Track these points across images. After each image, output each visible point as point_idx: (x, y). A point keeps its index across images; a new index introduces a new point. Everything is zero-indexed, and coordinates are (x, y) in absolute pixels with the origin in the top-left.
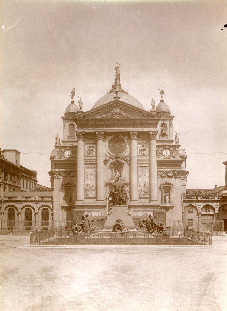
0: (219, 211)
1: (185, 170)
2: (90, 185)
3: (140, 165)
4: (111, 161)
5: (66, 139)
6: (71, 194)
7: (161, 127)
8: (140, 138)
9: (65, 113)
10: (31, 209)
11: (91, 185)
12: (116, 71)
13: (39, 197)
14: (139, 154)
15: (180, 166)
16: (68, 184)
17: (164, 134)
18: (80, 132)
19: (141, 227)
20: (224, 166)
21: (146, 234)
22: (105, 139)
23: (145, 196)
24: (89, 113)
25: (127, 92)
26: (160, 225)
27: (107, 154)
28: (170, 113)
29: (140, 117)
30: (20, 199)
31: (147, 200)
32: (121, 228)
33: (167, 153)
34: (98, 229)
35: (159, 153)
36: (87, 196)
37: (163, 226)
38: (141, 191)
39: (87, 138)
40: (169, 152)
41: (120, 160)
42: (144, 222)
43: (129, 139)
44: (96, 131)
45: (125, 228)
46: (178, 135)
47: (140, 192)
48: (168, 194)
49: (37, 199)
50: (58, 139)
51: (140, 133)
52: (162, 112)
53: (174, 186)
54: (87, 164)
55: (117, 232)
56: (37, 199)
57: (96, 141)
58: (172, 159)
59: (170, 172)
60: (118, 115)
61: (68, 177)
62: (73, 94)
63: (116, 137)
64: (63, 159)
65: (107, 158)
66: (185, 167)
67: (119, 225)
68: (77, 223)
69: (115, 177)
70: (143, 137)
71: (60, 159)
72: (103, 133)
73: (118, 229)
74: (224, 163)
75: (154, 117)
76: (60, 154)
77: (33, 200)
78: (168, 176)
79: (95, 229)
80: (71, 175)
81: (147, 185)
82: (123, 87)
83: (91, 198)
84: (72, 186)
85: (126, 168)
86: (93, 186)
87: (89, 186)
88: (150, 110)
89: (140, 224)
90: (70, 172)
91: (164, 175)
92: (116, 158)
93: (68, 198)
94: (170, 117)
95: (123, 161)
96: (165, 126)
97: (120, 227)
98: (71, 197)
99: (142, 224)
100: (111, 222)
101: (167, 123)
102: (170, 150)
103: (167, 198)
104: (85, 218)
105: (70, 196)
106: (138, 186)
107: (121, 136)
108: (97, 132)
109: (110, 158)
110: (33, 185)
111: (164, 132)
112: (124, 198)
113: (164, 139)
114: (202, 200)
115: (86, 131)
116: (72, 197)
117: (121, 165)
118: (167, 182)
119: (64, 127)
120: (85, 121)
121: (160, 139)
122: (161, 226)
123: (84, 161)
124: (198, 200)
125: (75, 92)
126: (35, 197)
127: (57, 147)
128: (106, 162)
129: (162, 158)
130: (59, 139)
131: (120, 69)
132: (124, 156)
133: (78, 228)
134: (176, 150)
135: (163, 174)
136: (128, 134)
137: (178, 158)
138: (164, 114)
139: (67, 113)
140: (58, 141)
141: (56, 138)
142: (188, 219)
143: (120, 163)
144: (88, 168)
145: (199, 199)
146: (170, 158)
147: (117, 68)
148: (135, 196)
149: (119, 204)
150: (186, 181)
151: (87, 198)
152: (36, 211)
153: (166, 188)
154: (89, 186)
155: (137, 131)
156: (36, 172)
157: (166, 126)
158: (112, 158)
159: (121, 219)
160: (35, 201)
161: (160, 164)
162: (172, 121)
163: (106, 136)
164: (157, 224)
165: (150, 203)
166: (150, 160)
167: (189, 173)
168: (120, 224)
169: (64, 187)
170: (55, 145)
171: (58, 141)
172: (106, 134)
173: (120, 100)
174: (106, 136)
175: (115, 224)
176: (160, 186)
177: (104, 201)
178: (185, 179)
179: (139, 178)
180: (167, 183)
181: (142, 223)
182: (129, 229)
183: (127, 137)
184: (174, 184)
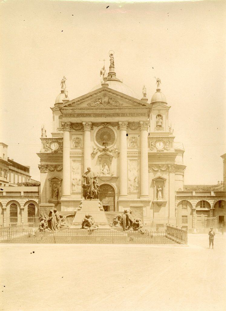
0: (215, 207)
1: (182, 164)
2: (76, 179)
3: (129, 158)
4: (99, 154)
5: (56, 132)
6: (58, 189)
7: (157, 118)
8: (130, 129)
9: (55, 103)
10: (17, 204)
11: (78, 180)
13: (24, 192)
14: (129, 147)
15: (174, 159)
16: (55, 178)
17: (160, 126)
18: (66, 122)
19: (115, 223)
20: (222, 160)
21: (118, 232)
22: (93, 130)
23: (136, 191)
24: (75, 101)
25: (121, 81)
26: (136, 221)
27: (95, 147)
28: (167, 103)
29: (130, 106)
30: (4, 194)
31: (136, 196)
32: (90, 224)
33: (160, 146)
34: (67, 225)
35: (152, 145)
36: (74, 192)
37: (140, 223)
39: (74, 129)
40: (162, 144)
41: (109, 153)
42: (119, 218)
43: (118, 129)
45: (95, 224)
47: (130, 186)
49: (22, 194)
50: (44, 131)
51: (129, 123)
52: (157, 102)
53: (167, 181)
55: (86, 229)
56: (22, 194)
57: (83, 132)
58: (165, 151)
59: (163, 165)
60: (106, 104)
61: (55, 171)
63: (104, 127)
64: (48, 152)
65: (95, 150)
66: (182, 161)
68: (44, 219)
69: (103, 171)
70: (133, 128)
71: (46, 152)
72: (90, 123)
73: (87, 225)
74: (222, 156)
75: (145, 105)
76: (47, 146)
77: (19, 195)
78: (161, 170)
79: (64, 226)
80: (58, 169)
82: (118, 77)
83: (77, 193)
85: (114, 162)
87: (75, 180)
88: (141, 98)
89: (114, 220)
90: (57, 166)
91: (156, 169)
92: (104, 150)
93: (55, 192)
94: (166, 108)
95: (111, 154)
97: (89, 223)
98: (58, 192)
99: (117, 220)
100: (80, 218)
101: (162, 113)
102: (164, 143)
103: (160, 193)
104: (53, 213)
105: (57, 191)
106: (128, 180)
107: (110, 127)
109: (98, 151)
110: (22, 179)
111: (160, 124)
113: (160, 131)
114: (197, 195)
116: (59, 192)
117: (110, 158)
119: (54, 118)
120: (71, 111)
121: (155, 131)
124: (193, 195)
126: (20, 192)
128: (93, 155)
129: (155, 151)
130: (46, 131)
132: (113, 148)
133: (44, 225)
134: (170, 142)
135: (155, 167)
136: (117, 124)
137: (172, 150)
138: (160, 104)
140: (44, 132)
142: (182, 216)
143: (109, 156)
144: (74, 161)
145: (194, 194)
146: (163, 151)
147: (112, 55)
148: (124, 191)
149: (91, 198)
150: (183, 176)
151: (73, 193)
152: (22, 207)
153: (159, 182)
154: (75, 180)
156: (29, 167)
158: (100, 151)
160: (21, 197)
161: (151, 157)
162: (168, 112)
163: (94, 126)
166: (140, 153)
167: (186, 168)
168: (89, 220)
169: (50, 182)
170: (41, 137)
171: (44, 132)
172: (93, 125)
173: (109, 87)
174: (94, 126)
175: (84, 221)
176: (153, 180)
178: (182, 174)
179: (129, 171)
180: (160, 178)
181: (117, 219)
182: (99, 225)
183: (116, 128)
184: (168, 179)
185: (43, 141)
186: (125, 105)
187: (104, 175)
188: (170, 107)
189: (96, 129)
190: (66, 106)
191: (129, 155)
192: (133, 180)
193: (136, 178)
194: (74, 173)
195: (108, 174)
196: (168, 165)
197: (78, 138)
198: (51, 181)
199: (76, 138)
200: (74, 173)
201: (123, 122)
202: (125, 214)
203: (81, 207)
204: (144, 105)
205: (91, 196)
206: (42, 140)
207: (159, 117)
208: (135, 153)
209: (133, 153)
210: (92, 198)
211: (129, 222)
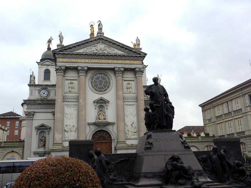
11: (72, 125)
12: (90, 28)
23: (133, 137)
34: (120, 179)
44: (78, 66)
46: (160, 76)
50: (32, 77)
62: (50, 41)
67: (176, 168)
81: (135, 125)
84: (47, 129)
86: (74, 126)
87: (69, 126)
104: (96, 157)
108: (79, 66)
117: (106, 103)
123: (64, 98)
125: (51, 41)
130: (34, 78)
131: (94, 26)
139: (43, 59)
141: (31, 76)
155: (123, 67)
159: (180, 156)
169: (37, 130)
171: (32, 77)
185: (31, 88)
186: (120, 53)
187: (100, 121)
188: (147, 66)
189: (89, 75)
194: (68, 119)
195: (104, 119)
197: (72, 83)
198: (38, 129)
199: (70, 83)
200: (67, 119)
201: (119, 68)
202: (216, 154)
203: (151, 142)
204: (139, 54)
205: (165, 125)
206: (30, 87)
208: (132, 98)
209: (129, 99)
211: (227, 168)
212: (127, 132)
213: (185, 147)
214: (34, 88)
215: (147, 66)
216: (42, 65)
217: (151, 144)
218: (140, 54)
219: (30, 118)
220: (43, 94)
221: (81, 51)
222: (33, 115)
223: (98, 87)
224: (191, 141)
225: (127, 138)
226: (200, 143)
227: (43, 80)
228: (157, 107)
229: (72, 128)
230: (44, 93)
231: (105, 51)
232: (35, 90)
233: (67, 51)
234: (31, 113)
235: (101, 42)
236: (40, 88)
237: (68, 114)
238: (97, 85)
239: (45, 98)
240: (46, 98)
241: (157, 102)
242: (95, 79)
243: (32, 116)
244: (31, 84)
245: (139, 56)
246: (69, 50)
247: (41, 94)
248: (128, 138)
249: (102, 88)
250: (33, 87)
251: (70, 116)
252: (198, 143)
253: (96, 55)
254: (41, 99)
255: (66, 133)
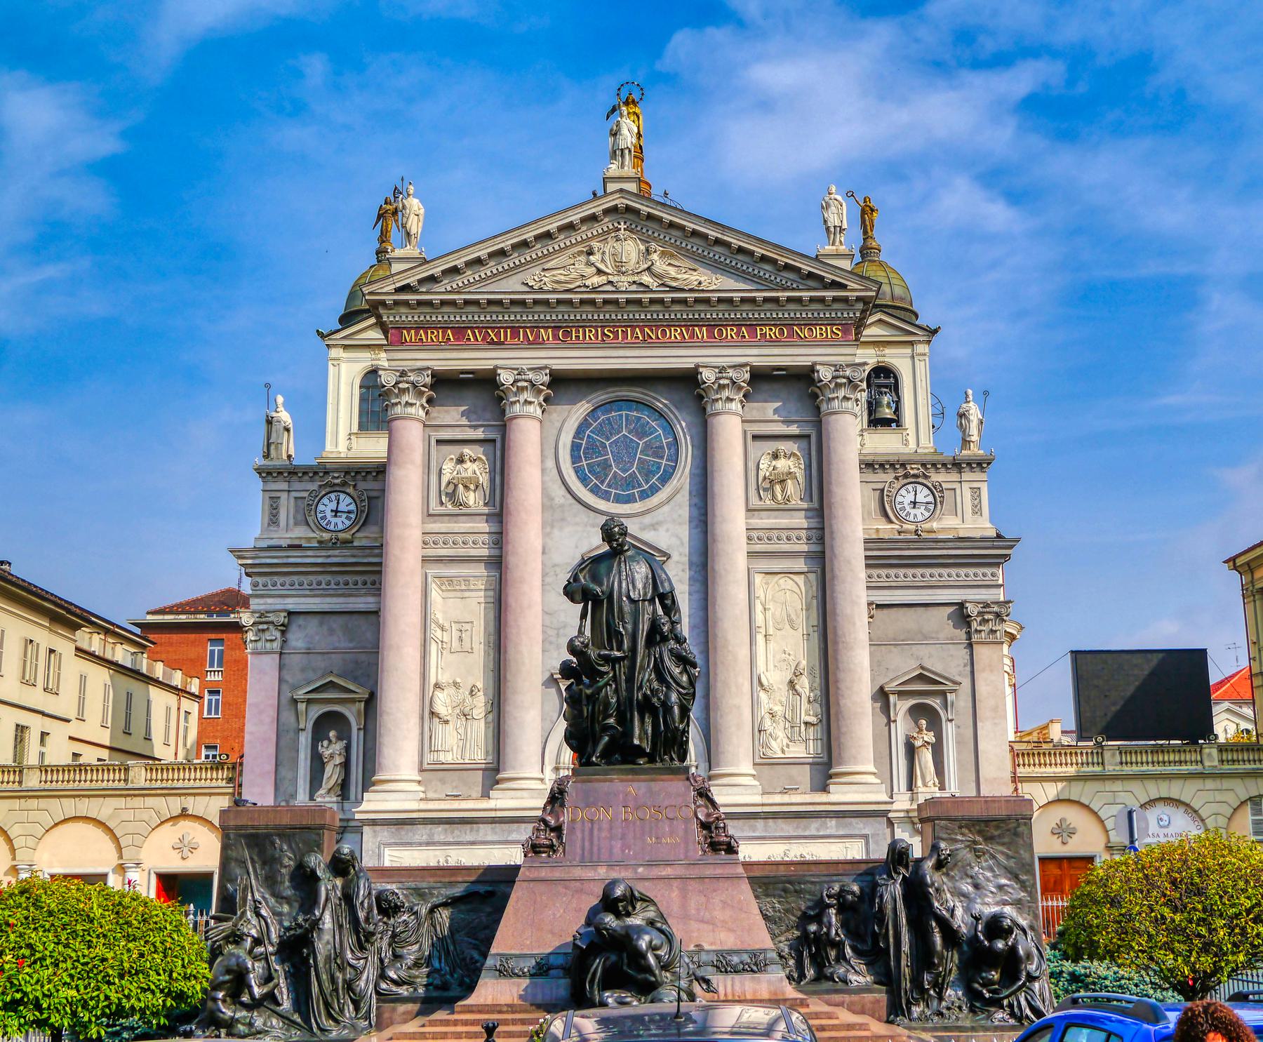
23: (798, 751)
24: (460, 263)
31: (804, 775)
32: (648, 969)
38: (772, 715)
48: (930, 737)
53: (960, 700)
54: (439, 560)
60: (631, 279)
73: (613, 980)
84: (353, 701)
96: (892, 380)
97: (637, 957)
111: (887, 413)
112: (674, 697)
115: (439, 366)
118: (922, 668)
122: (1000, 945)
123: (425, 543)
127: (269, 473)
157: (896, 378)
164: (961, 921)
165: (832, 788)
177: (542, 780)
182: (718, 980)
188: (935, 332)
190: (406, 288)
191: (759, 548)
192: (785, 687)
193: (797, 674)
196: (961, 605)
198: (309, 701)
201: (722, 370)
205: (636, 742)
207: (882, 381)
210: (639, 751)
212: (768, 723)
213: (714, 846)
214: (284, 486)
215: (935, 332)
216: (346, 347)
217: (558, 830)
218: (843, 287)
219: (268, 645)
220: (329, 517)
221: (511, 286)
222: (284, 629)
223: (607, 476)
224: (1159, 769)
225: (765, 756)
226: (1210, 784)
227: (355, 428)
228: (607, 659)
229: (469, 700)
230: (336, 512)
231: (646, 279)
232: (294, 494)
233: (439, 288)
234: (272, 618)
235: (622, 226)
236: (314, 486)
237: (447, 625)
238: (606, 466)
239: (341, 535)
240: (347, 536)
241: (614, 636)
242: (599, 431)
243: (278, 634)
244: (275, 463)
245: (835, 299)
246: (446, 284)
247: (324, 518)
248: (770, 754)
249: (631, 482)
250: (281, 477)
251: (455, 634)
252: (1198, 784)
253: (592, 302)
254: (320, 542)
255: (436, 720)
